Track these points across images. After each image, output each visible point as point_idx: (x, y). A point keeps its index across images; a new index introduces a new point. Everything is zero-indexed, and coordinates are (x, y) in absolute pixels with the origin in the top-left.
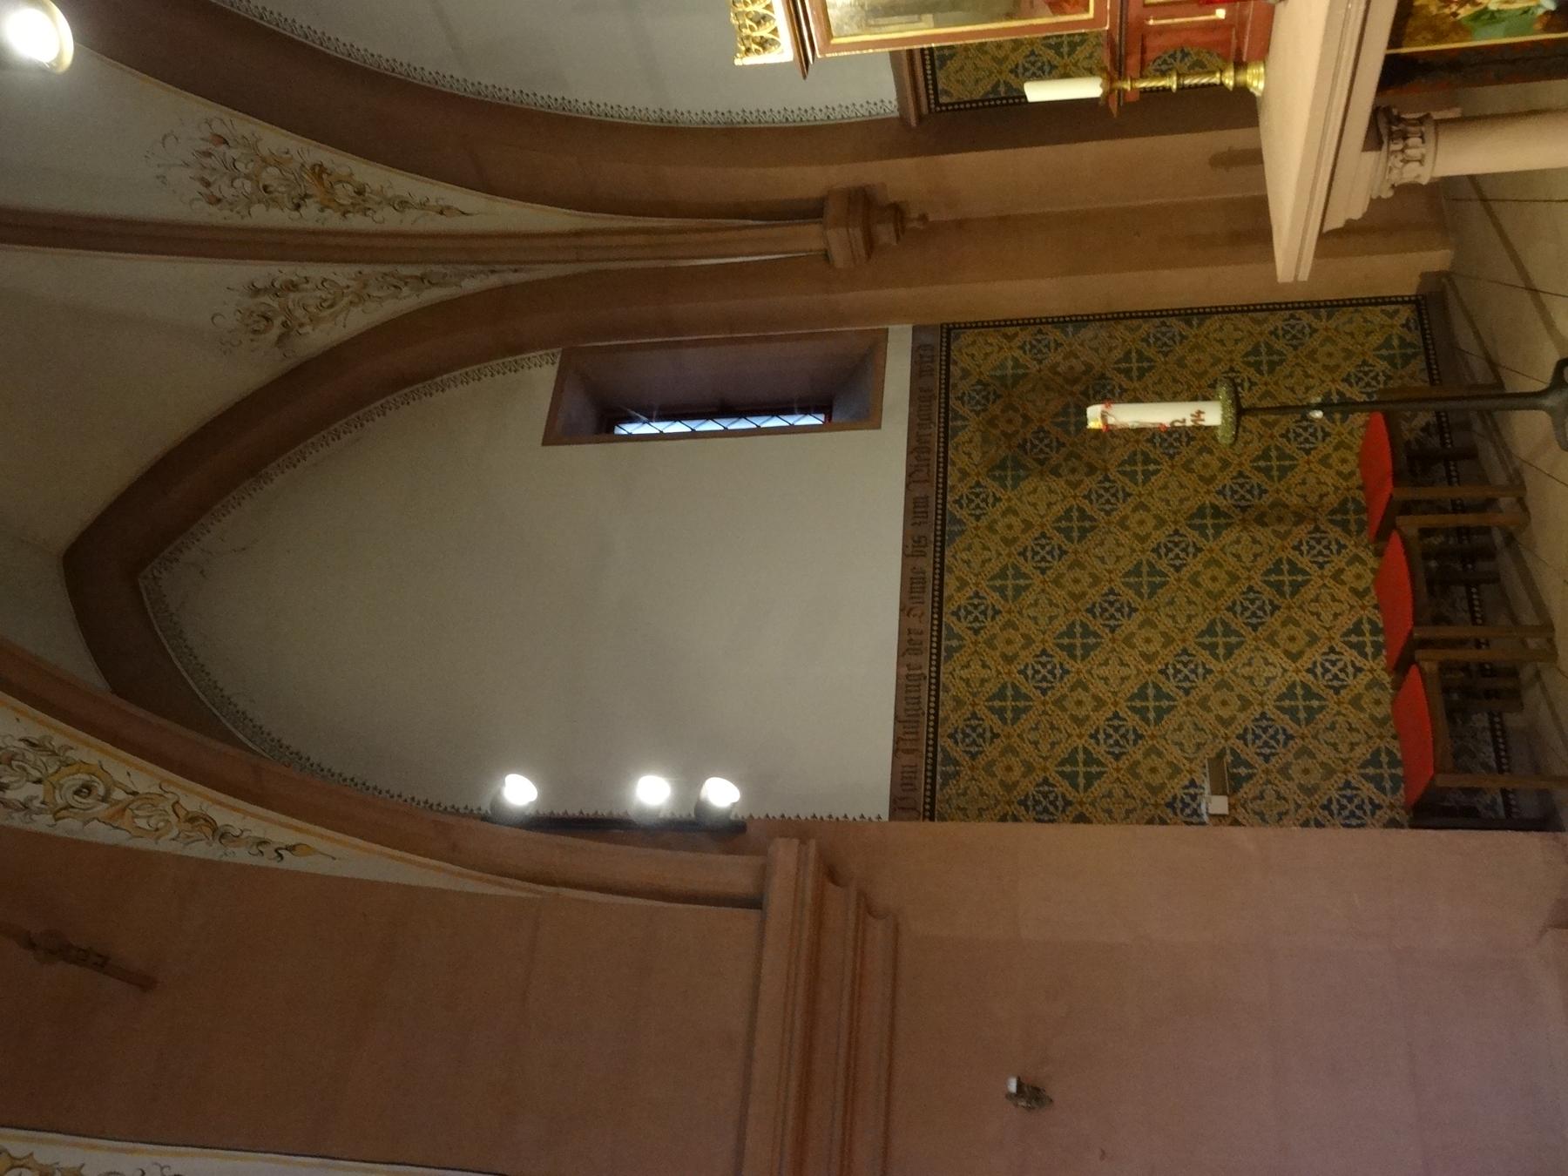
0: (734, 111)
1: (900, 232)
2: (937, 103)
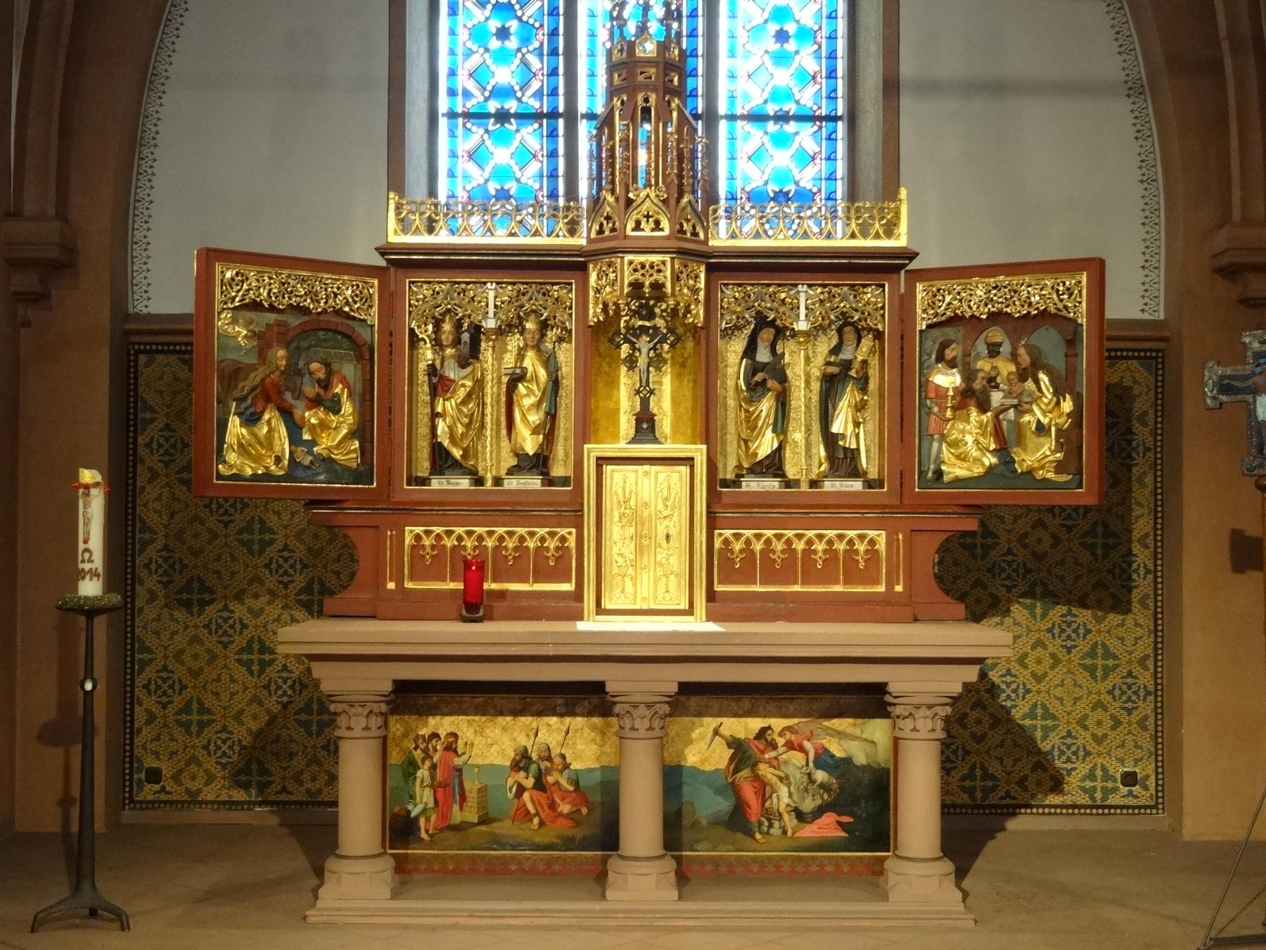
0: (156, 151)
2: (138, 352)
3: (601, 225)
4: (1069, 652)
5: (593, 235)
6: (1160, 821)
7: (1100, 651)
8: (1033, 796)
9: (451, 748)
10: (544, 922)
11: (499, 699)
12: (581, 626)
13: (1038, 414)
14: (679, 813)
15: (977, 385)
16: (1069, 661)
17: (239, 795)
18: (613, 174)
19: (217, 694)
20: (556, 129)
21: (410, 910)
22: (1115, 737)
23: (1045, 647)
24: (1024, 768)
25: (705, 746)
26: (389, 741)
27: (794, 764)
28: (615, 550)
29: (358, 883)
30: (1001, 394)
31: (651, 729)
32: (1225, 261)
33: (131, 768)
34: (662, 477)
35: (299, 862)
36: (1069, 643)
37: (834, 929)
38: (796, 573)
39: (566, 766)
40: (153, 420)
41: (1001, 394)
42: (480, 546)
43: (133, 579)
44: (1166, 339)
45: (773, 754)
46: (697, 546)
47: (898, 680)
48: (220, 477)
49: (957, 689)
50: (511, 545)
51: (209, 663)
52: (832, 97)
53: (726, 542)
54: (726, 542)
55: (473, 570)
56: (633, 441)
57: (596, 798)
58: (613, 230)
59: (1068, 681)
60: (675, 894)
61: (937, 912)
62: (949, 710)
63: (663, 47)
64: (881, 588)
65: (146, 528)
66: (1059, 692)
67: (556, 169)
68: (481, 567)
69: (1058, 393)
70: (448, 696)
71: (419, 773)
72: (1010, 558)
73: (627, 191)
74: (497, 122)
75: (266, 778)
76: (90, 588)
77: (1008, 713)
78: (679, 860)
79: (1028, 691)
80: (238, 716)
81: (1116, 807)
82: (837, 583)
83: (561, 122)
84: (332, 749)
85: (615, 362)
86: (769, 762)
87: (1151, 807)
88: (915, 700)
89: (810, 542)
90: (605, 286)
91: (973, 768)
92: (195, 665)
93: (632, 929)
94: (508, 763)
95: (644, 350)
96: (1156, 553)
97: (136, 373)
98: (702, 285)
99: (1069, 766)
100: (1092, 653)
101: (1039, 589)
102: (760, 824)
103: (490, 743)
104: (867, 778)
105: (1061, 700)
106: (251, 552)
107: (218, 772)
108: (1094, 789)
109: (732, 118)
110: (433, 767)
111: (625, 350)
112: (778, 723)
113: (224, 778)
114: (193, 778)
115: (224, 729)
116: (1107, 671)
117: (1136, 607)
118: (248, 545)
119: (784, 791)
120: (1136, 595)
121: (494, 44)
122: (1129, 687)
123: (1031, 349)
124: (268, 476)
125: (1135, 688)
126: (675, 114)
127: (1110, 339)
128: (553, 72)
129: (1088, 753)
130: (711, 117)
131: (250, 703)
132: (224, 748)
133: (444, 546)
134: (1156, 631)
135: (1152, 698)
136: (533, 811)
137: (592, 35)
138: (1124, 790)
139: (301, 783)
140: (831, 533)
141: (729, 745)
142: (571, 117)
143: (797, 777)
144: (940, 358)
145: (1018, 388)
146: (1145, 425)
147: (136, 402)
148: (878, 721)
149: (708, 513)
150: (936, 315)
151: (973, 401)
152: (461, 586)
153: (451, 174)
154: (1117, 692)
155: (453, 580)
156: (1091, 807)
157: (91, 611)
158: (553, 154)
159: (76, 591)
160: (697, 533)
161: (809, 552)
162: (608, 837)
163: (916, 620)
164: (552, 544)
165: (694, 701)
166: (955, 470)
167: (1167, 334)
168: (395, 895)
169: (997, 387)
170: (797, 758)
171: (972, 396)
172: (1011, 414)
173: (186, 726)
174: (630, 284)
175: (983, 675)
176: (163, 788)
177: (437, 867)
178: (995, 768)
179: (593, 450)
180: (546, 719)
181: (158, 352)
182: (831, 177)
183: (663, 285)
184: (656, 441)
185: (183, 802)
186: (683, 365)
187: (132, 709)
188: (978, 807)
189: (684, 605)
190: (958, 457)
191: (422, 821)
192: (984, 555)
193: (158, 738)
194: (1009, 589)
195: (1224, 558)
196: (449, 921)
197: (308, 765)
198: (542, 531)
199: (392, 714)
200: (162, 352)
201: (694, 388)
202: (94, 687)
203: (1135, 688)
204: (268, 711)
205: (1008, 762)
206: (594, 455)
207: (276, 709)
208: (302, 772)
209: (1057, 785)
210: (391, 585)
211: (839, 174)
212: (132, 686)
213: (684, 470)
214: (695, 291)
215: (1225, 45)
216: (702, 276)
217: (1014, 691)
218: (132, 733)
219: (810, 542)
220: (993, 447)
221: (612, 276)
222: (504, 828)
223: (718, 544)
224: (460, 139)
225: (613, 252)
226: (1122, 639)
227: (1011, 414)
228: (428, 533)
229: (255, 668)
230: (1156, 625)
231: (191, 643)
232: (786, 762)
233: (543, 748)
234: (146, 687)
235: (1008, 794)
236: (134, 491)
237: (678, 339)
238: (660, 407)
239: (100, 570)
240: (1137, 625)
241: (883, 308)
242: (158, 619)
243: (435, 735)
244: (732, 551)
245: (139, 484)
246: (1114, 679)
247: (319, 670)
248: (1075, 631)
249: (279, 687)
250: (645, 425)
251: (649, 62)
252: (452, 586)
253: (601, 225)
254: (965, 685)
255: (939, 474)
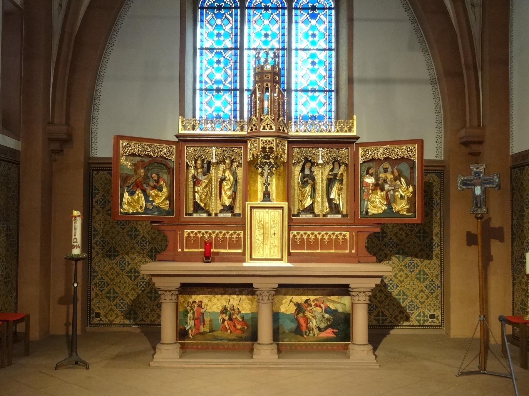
1: (54, 152)
2: (94, 170)
3: (252, 128)
4: (411, 273)
5: (249, 131)
6: (442, 331)
7: (422, 273)
8: (399, 322)
9: (200, 306)
10: (231, 366)
11: (216, 289)
12: (245, 264)
13: (401, 192)
14: (278, 329)
15: (380, 182)
16: (412, 276)
17: (127, 322)
18: (256, 110)
19: (119, 287)
20: (236, 94)
21: (186, 362)
22: (427, 302)
23: (403, 271)
24: (396, 313)
25: (287, 305)
26: (179, 304)
27: (318, 311)
28: (256, 238)
29: (168, 352)
30: (388, 185)
31: (268, 300)
32: (464, 140)
33: (90, 312)
34: (272, 213)
35: (148, 345)
36: (411, 270)
37: (332, 369)
38: (318, 246)
39: (239, 312)
40: (98, 193)
41: (388, 185)
42: (210, 237)
43: (91, 248)
44: (444, 166)
45: (310, 308)
46: (284, 237)
47: (353, 283)
48: (121, 213)
49: (373, 286)
50: (221, 236)
51: (117, 276)
52: (330, 84)
53: (294, 235)
54: (294, 235)
55: (208, 245)
56: (263, 201)
57: (250, 323)
58: (256, 129)
59: (411, 283)
60: (277, 357)
61: (367, 363)
62: (370, 293)
63: (273, 67)
64: (347, 251)
65: (95, 230)
66: (408, 287)
67: (236, 108)
68: (211, 244)
69: (408, 185)
70: (199, 288)
71: (189, 315)
72: (391, 241)
73: (261, 116)
74: (216, 92)
75: (136, 316)
76: (76, 251)
77: (391, 294)
78: (278, 344)
79: (398, 286)
80: (127, 295)
81: (427, 326)
82: (332, 249)
83: (238, 92)
84: (159, 306)
85: (256, 174)
86: (309, 311)
87: (440, 326)
88: (359, 290)
89: (323, 236)
90: (253, 148)
91: (379, 313)
92: (112, 277)
93: (262, 368)
94: (219, 311)
95: (267, 170)
96: (441, 239)
97: (92, 177)
98: (286, 148)
99: (411, 312)
100: (419, 273)
101: (401, 251)
102: (306, 332)
103: (213, 304)
104: (342, 317)
105: (409, 289)
106: (131, 238)
107: (120, 313)
108: (420, 320)
109: (296, 91)
110: (194, 313)
111: (260, 170)
112: (312, 298)
113: (122, 316)
114: (111, 316)
115: (122, 299)
116: (424, 279)
117: (434, 258)
118: (130, 236)
119: (314, 321)
120: (434, 254)
121: (215, 65)
122: (432, 285)
123: (398, 170)
124: (137, 213)
125: (434, 285)
126: (277, 90)
127: (425, 166)
128: (236, 75)
129: (418, 308)
130: (289, 91)
131: (131, 290)
132: (122, 305)
133: (198, 237)
134: (441, 266)
135: (440, 289)
136: (228, 328)
137: (249, 63)
138: (430, 320)
139: (148, 318)
140: (330, 233)
141: (295, 305)
142: (242, 90)
143: (319, 316)
144: (367, 173)
145: (394, 183)
146: (437, 195)
147: (92, 187)
148: (346, 297)
149: (288, 225)
150: (366, 158)
151: (378, 188)
152: (203, 250)
153: (201, 110)
154: (428, 287)
155: (201, 248)
156: (419, 326)
157: (76, 259)
158: (235, 103)
159: (72, 251)
160: (284, 232)
161: (323, 239)
162: (254, 337)
163: (359, 262)
164: (235, 236)
165: (283, 290)
166: (372, 211)
167: (444, 165)
168: (181, 357)
169: (387, 183)
170: (319, 310)
171: (378, 186)
172: (392, 192)
173: (109, 298)
174: (262, 148)
175: (382, 281)
176: (101, 320)
177: (195, 347)
178: (386, 313)
179: (249, 204)
180: (233, 296)
182: (330, 111)
183: (273, 148)
184: (270, 201)
185: (108, 324)
186: (280, 175)
187: (90, 292)
188: (381, 326)
189: (280, 257)
190: (374, 207)
191: (190, 331)
192: (382, 240)
193: (99, 302)
194: (391, 252)
195: (464, 241)
196: (200, 366)
197: (151, 311)
198: (231, 232)
199: (180, 294)
200: (102, 170)
201: (283, 183)
202: (77, 285)
203: (434, 285)
204: (137, 293)
205: (391, 311)
206: (249, 206)
207: (140, 292)
208: (149, 314)
209: (407, 318)
210: (180, 250)
211: (333, 110)
212: (91, 284)
213: (280, 211)
214: (284, 150)
215: (464, 67)
216: (286, 145)
217: (393, 286)
218: (90, 300)
219: (323, 236)
220: (385, 203)
221: (255, 145)
222: (218, 334)
223: (291, 236)
224: (204, 98)
225: (256, 137)
226: (429, 268)
227: (392, 192)
228: (192, 232)
229: (133, 278)
230: (441, 264)
231: (110, 270)
232: (315, 311)
233: (232, 306)
234: (95, 284)
235: (391, 321)
236: (92, 217)
237: (278, 166)
238: (272, 189)
239: (80, 245)
240: (435, 264)
241: (348, 156)
242: (100, 261)
243: (195, 302)
244: (296, 239)
245: (92, 298)
246: (427, 282)
247: (155, 280)
248: (414, 266)
249: (141, 285)
250: (267, 196)
251: (268, 72)
252: (200, 250)
253: (252, 128)
254: (376, 285)
255: (367, 212)
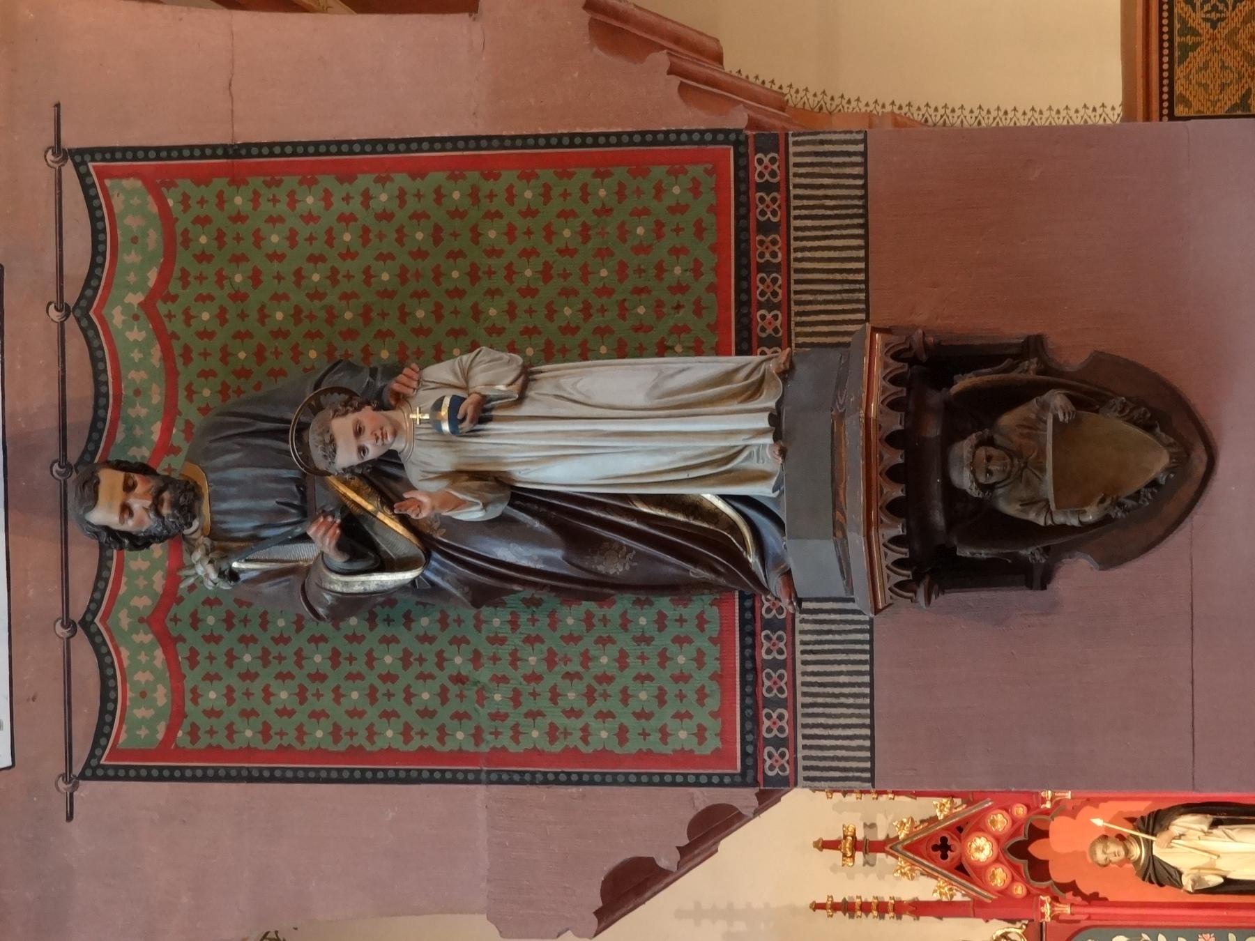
181: (1171, 92)
200: (1171, 85)
